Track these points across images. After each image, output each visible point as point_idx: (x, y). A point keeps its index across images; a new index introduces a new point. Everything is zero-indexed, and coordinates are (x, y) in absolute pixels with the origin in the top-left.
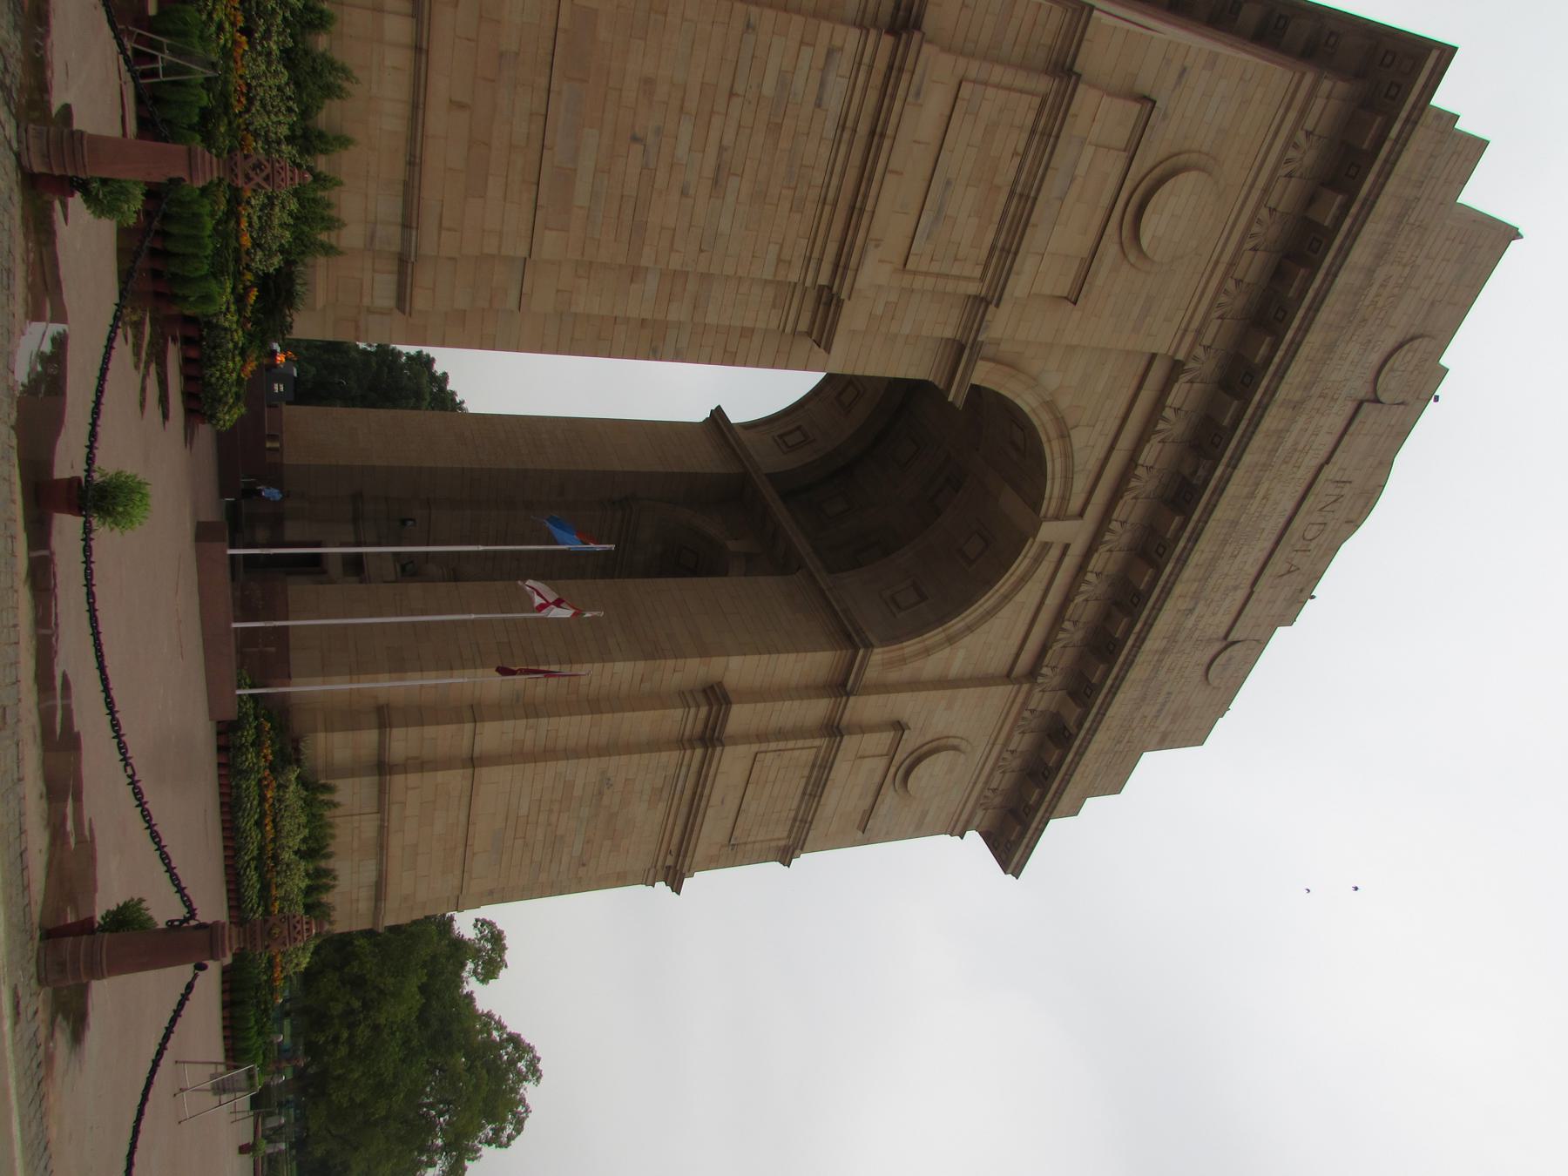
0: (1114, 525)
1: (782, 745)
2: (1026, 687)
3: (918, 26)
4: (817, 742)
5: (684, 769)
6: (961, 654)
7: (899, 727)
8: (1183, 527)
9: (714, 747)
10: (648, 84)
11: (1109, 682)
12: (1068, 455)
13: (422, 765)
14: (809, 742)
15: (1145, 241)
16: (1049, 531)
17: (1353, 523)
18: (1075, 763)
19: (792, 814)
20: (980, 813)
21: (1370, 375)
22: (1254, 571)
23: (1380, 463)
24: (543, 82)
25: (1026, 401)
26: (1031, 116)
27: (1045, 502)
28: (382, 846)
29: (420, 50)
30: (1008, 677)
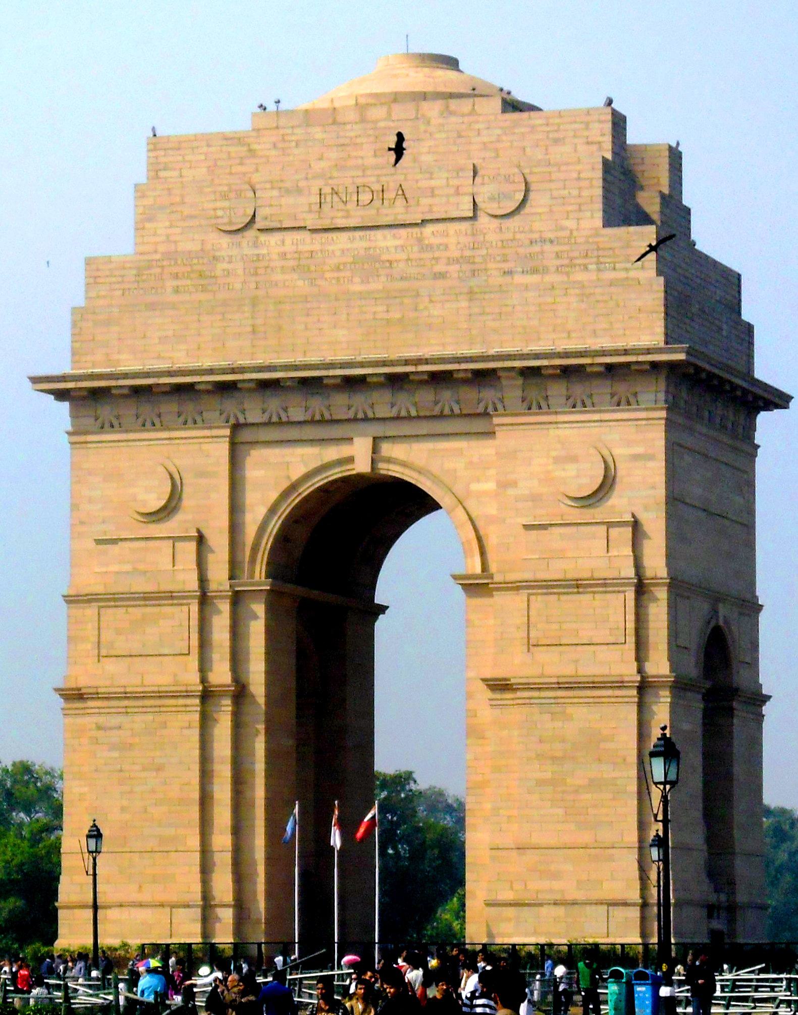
0: (351, 415)
3: (80, 689)
5: (532, 701)
6: (474, 487)
10: (123, 809)
11: (464, 366)
12: (307, 477)
15: (162, 503)
16: (362, 466)
21: (238, 238)
22: (403, 232)
23: (334, 122)
24: (128, 854)
25: (275, 526)
28: (574, 903)
29: (121, 906)
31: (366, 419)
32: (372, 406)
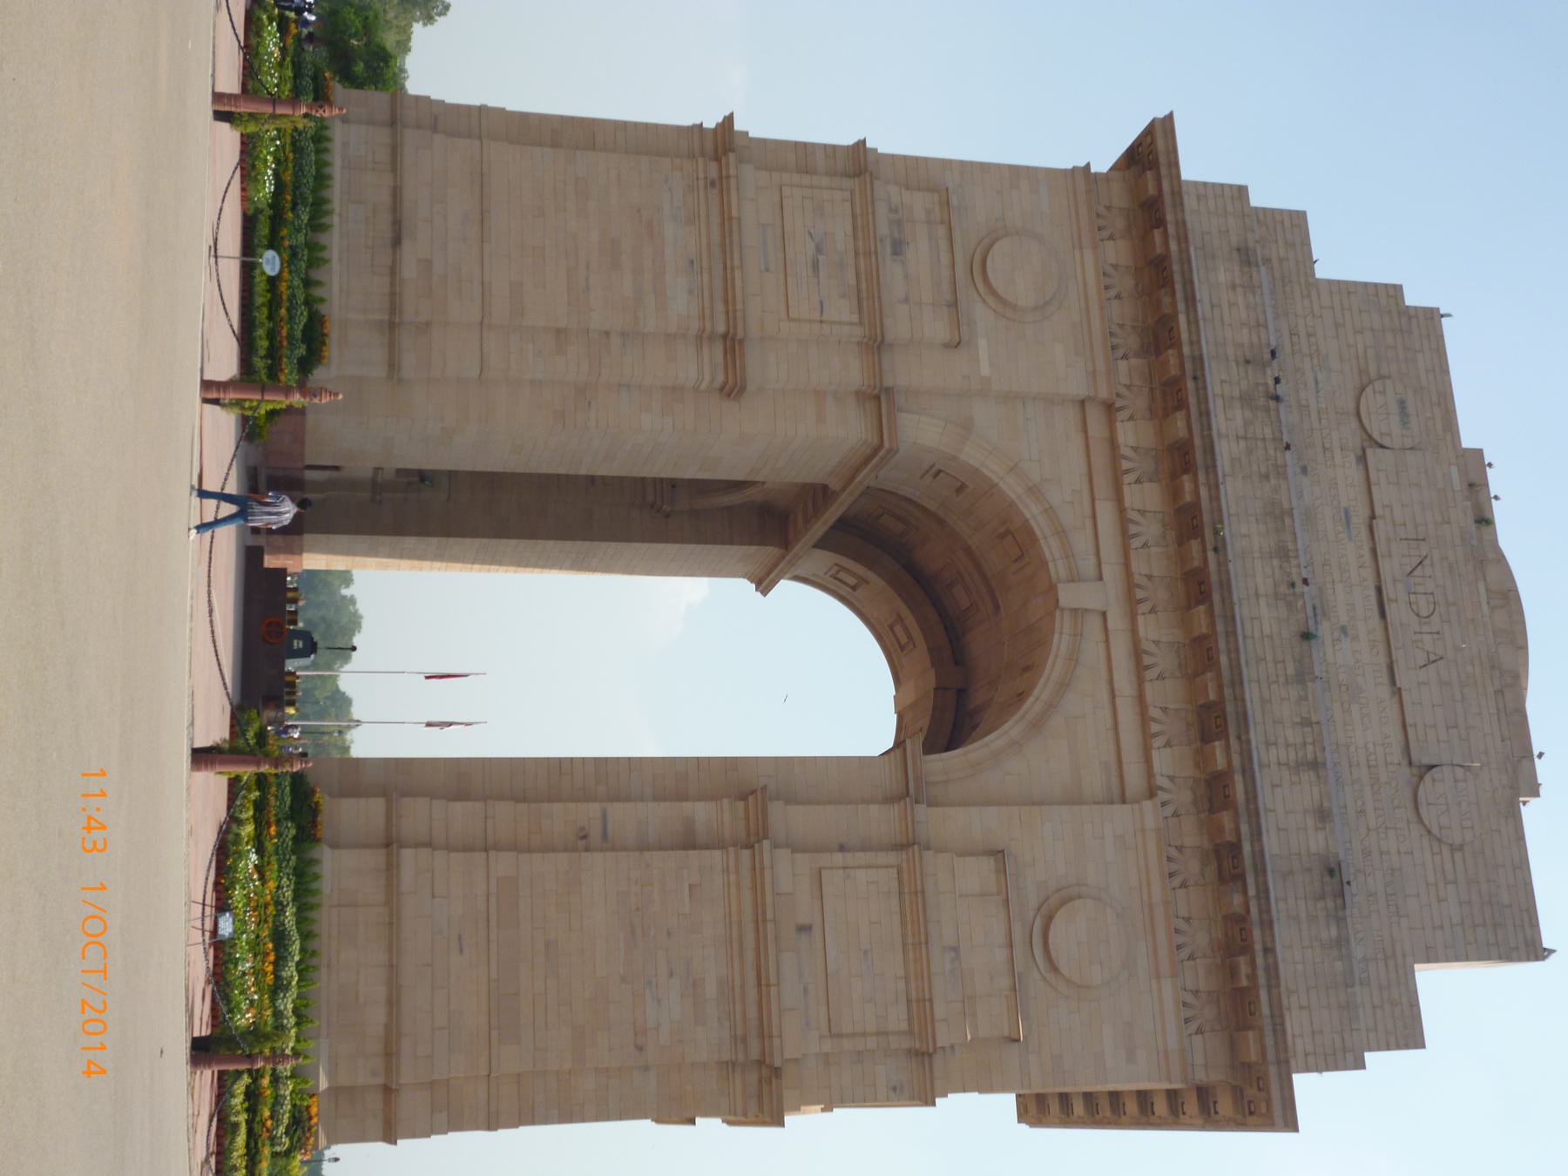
1: (849, 859)
2: (1148, 804)
4: (892, 858)
7: (999, 854)
8: (1204, 551)
9: (759, 841)
13: (429, 845)
14: (882, 858)
15: (1000, 291)
16: (1068, 596)
17: (1513, 635)
18: (1263, 892)
19: (901, 986)
20: (1198, 1039)
26: (848, 205)
27: (1051, 565)
30: (1124, 802)
31: (1132, 603)
32: (1153, 611)
